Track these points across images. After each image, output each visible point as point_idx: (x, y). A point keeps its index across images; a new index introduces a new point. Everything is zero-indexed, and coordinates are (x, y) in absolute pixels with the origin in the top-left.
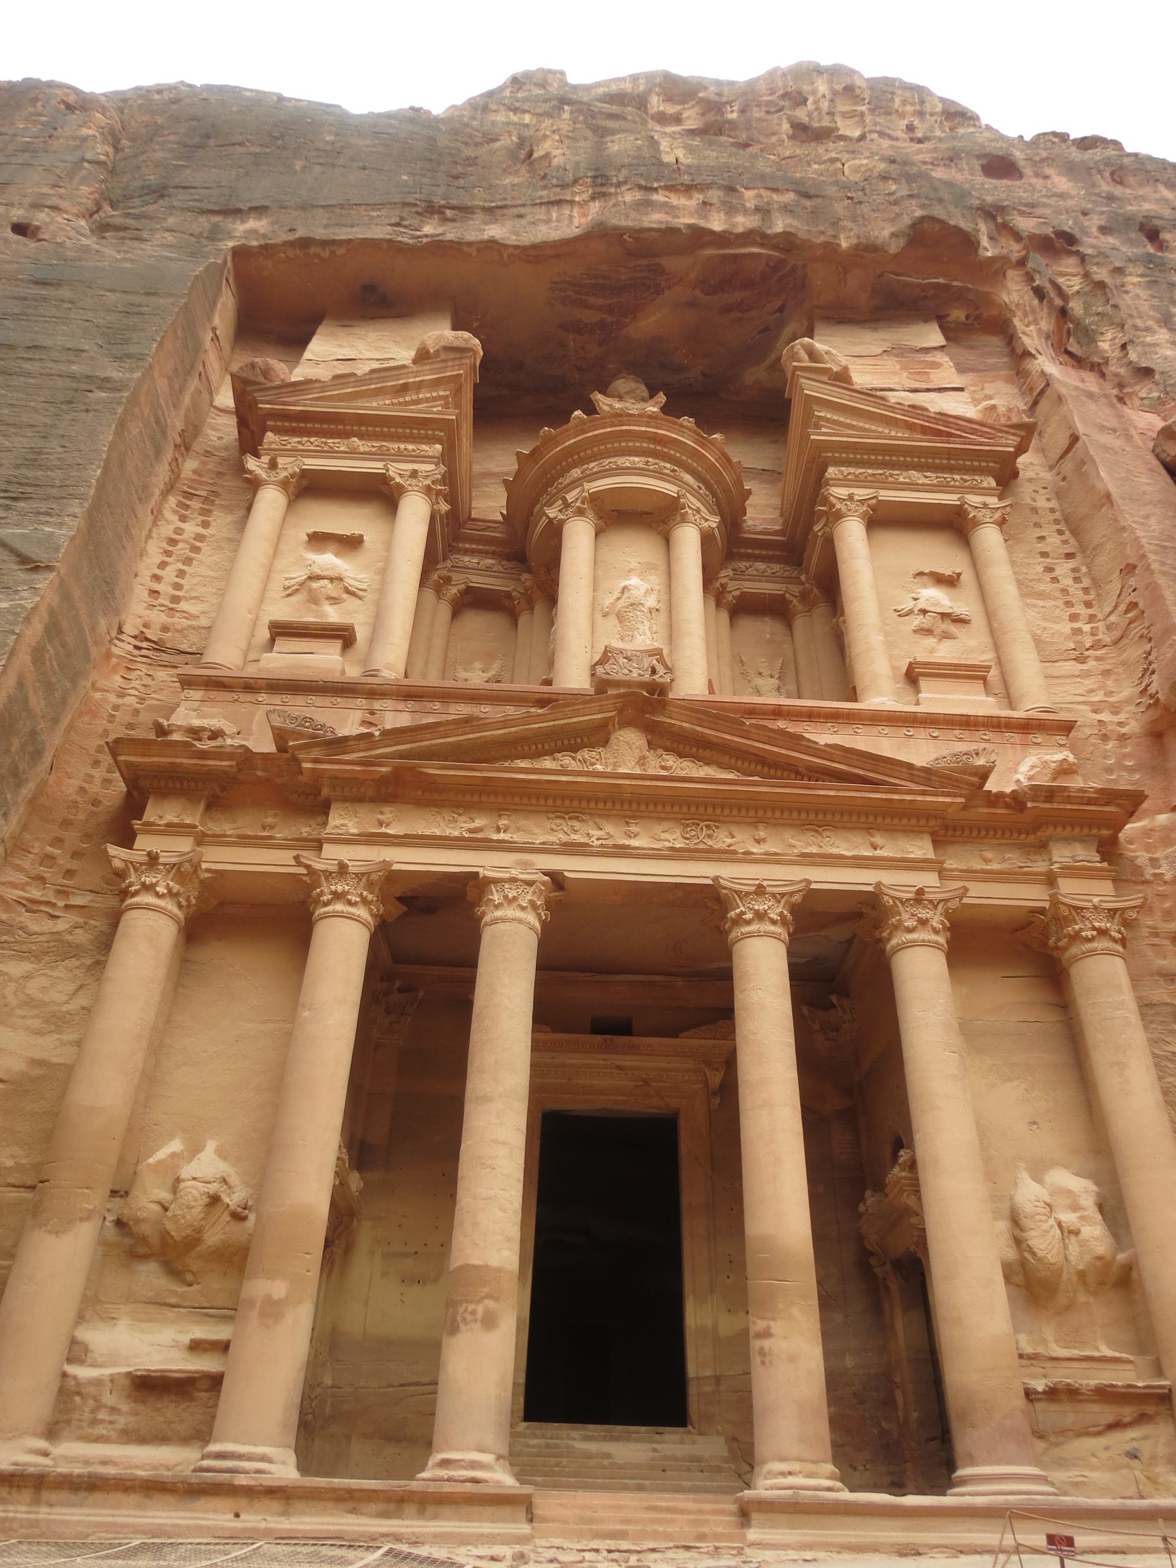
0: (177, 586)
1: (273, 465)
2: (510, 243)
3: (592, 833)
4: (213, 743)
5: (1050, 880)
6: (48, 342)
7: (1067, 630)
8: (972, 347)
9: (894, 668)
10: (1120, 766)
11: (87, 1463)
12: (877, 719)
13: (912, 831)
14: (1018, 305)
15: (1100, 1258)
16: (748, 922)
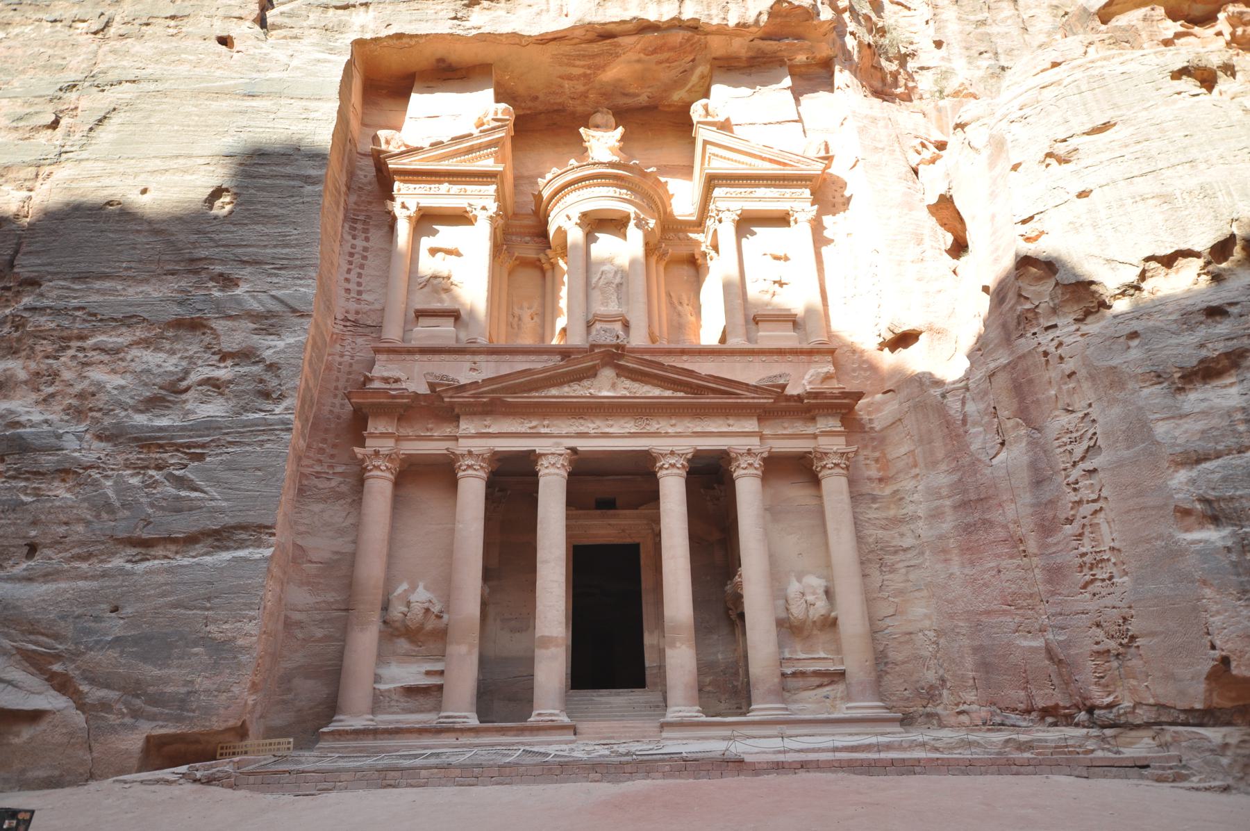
0: (359, 284)
1: (404, 206)
3: (589, 426)
4: (395, 386)
9: (746, 316)
11: (390, 723)
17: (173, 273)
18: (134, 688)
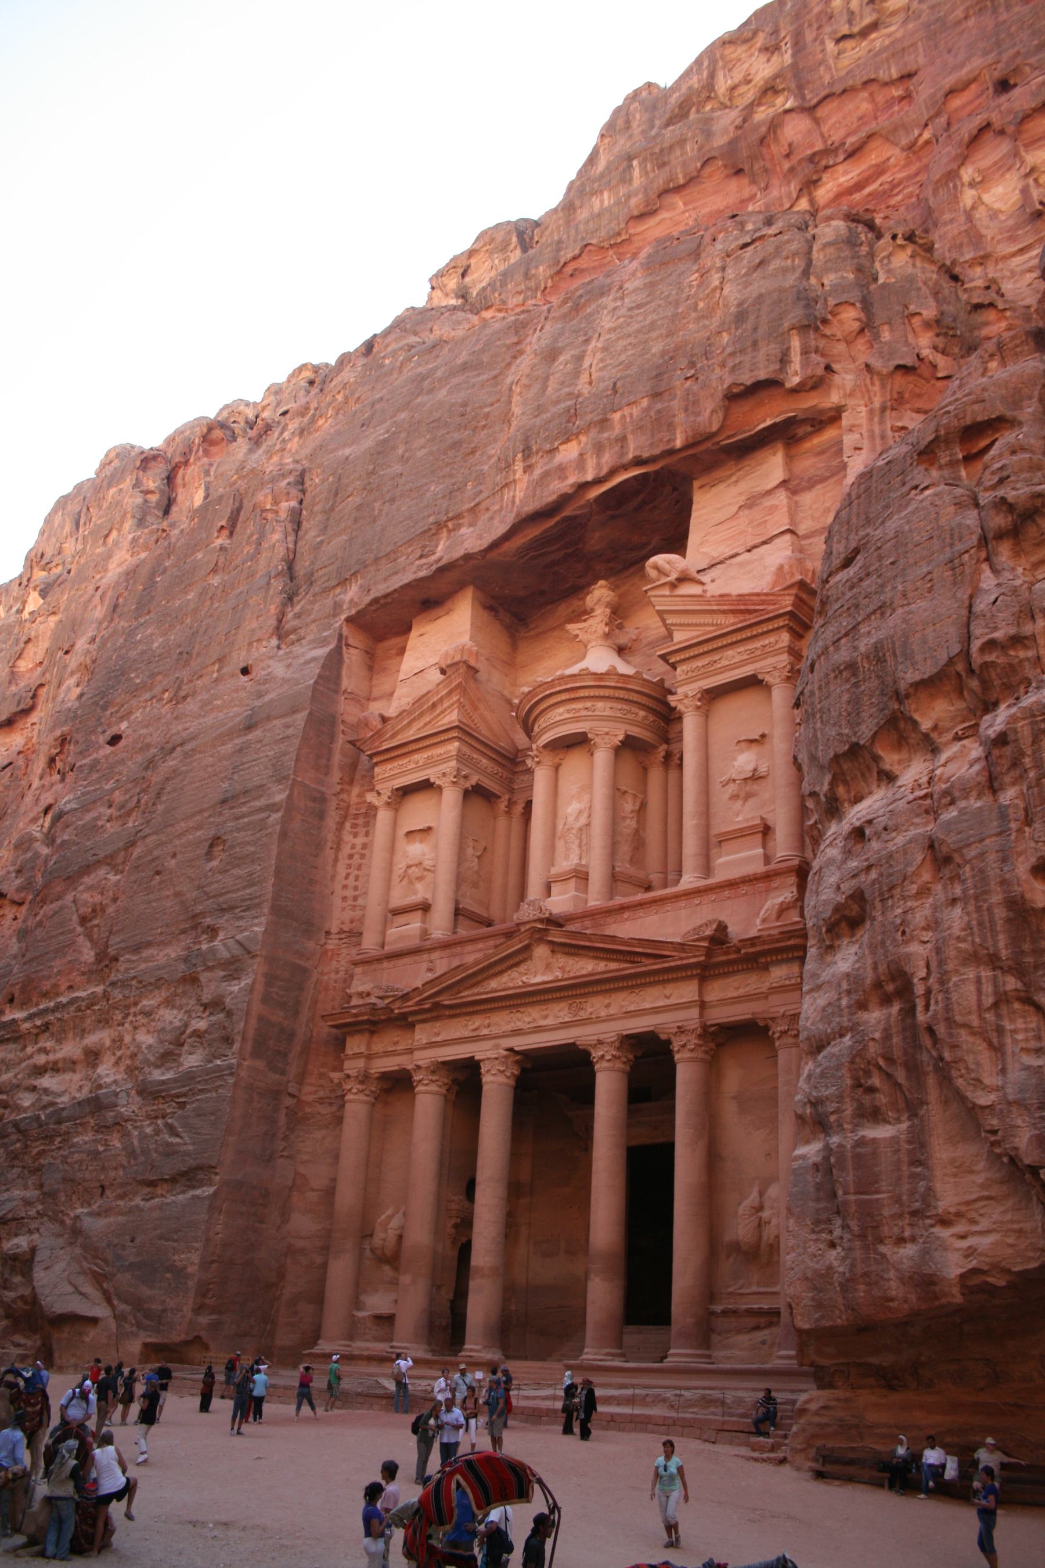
1: (379, 794)
2: (476, 550)
6: (250, 786)
8: (822, 452)
12: (677, 897)
14: (851, 395)
17: (184, 932)
18: (138, 1304)
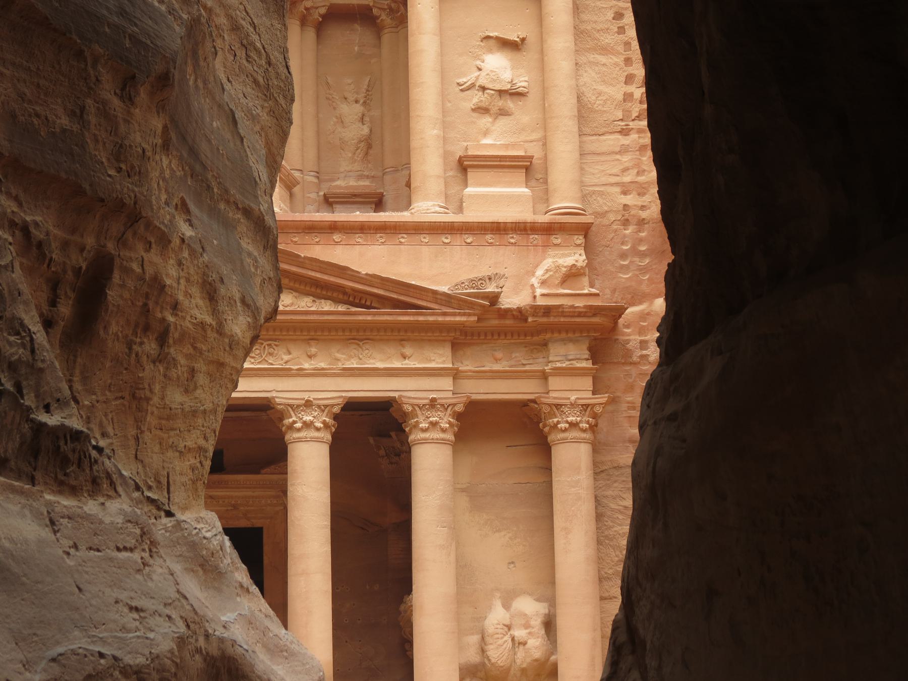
5: (544, 376)
7: (620, 97)
9: (446, 155)
10: (635, 251)
13: (437, 340)
15: (536, 660)
16: (299, 430)
